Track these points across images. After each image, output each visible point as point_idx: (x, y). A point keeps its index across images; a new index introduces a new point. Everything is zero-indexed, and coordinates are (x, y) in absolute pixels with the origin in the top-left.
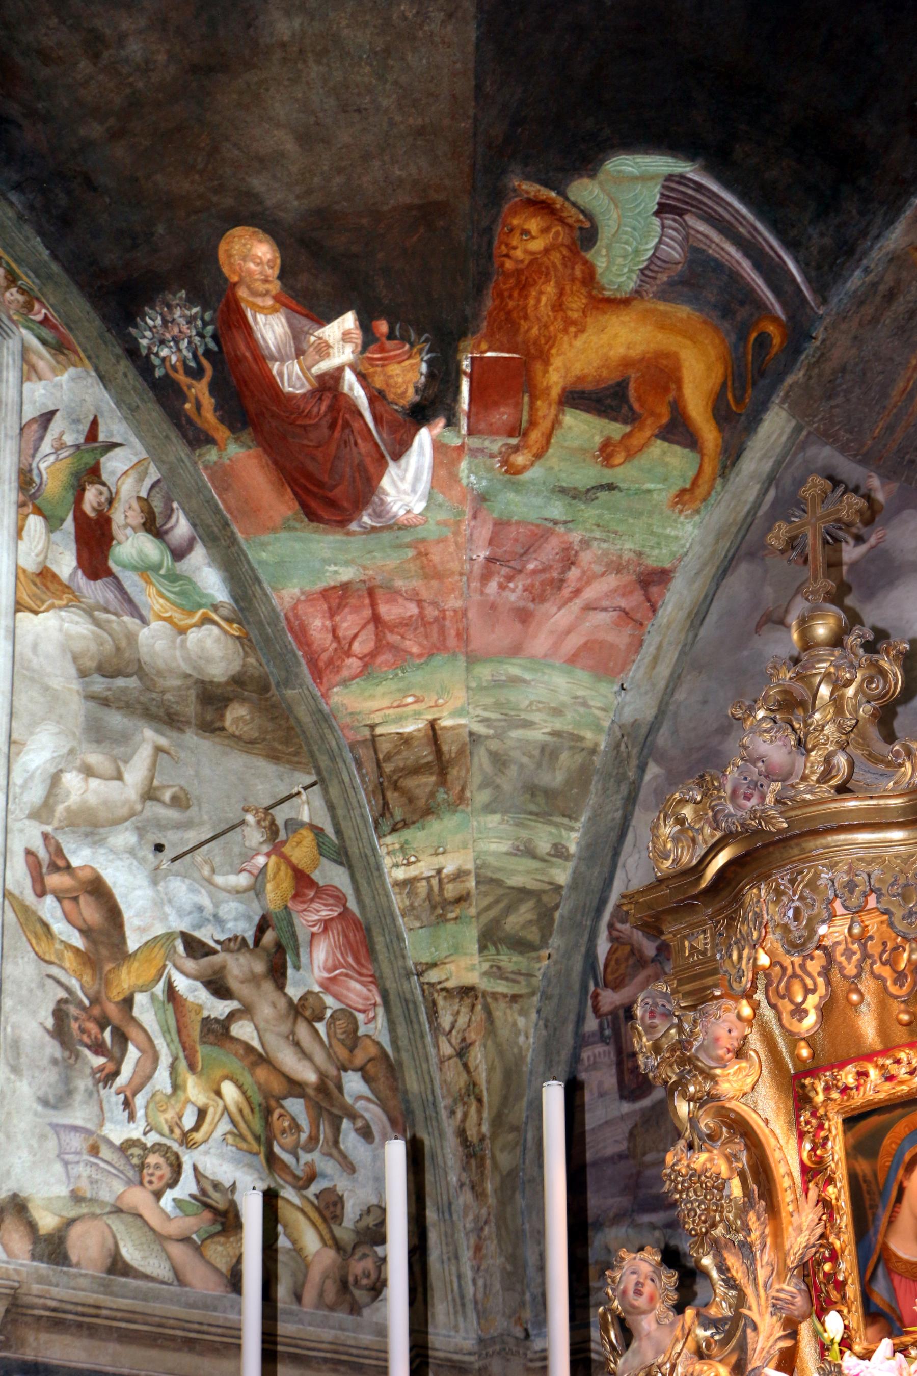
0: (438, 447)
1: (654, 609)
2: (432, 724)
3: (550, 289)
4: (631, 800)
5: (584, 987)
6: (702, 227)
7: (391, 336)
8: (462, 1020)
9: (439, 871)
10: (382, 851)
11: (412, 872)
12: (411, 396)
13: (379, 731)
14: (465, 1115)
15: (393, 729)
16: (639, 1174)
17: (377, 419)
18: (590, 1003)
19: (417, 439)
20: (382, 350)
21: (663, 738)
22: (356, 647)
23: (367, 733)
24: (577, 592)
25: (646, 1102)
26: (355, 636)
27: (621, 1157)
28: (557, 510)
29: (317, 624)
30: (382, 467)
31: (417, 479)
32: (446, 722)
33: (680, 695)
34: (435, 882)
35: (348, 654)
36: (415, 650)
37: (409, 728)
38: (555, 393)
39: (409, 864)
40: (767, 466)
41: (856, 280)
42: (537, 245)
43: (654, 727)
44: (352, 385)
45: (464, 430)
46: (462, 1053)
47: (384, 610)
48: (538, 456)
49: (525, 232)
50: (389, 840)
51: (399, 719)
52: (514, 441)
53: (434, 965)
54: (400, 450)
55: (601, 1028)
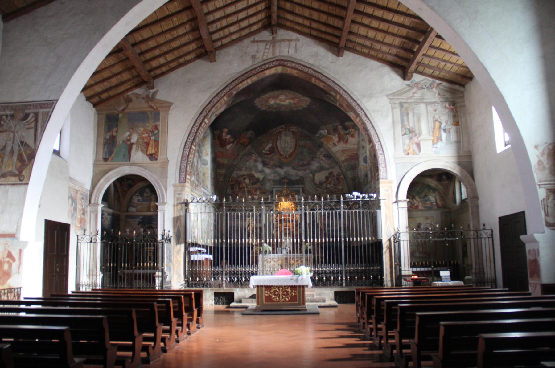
0: (232, 146)
44: (228, 140)
54: (229, 144)
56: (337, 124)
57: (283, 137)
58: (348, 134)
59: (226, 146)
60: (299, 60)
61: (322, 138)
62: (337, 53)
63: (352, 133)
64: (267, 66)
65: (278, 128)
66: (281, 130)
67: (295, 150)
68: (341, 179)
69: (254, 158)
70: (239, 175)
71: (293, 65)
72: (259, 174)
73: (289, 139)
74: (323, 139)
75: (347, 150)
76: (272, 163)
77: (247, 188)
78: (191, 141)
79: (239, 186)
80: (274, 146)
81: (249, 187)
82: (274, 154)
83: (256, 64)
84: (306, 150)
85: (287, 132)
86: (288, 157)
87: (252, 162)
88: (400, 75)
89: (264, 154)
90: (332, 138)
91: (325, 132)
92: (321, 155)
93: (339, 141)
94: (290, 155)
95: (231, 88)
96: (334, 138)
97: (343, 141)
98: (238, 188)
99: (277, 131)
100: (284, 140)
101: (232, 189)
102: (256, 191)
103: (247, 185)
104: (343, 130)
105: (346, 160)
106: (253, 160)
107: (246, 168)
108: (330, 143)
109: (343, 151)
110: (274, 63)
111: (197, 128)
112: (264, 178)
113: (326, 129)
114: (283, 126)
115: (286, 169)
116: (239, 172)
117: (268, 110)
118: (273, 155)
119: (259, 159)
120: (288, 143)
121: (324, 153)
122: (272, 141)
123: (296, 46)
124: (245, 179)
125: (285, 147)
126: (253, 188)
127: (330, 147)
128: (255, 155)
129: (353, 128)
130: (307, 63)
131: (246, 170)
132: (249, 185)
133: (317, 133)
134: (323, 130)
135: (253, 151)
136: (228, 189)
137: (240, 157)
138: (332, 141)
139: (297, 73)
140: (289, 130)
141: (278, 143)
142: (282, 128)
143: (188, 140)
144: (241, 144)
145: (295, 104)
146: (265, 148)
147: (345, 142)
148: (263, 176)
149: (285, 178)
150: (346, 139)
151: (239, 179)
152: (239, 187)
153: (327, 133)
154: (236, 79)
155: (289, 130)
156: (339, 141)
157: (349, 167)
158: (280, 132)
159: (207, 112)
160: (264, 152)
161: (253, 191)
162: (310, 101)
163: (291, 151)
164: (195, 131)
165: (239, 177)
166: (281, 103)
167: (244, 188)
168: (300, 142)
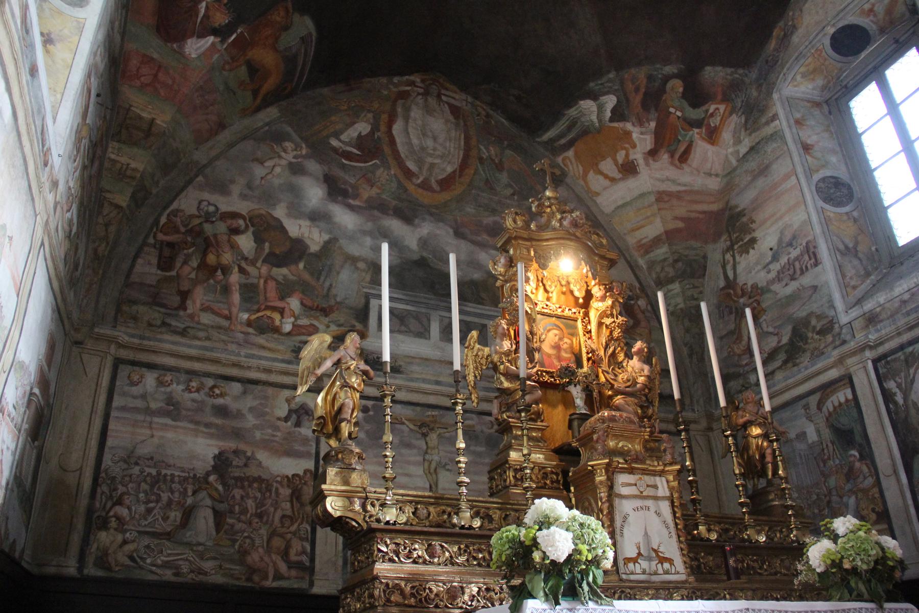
0: (213, 44)
1: (216, 135)
2: (153, 119)
3: (270, 32)
4: (190, 182)
5: (151, 229)
6: (303, 51)
7: (225, 5)
8: (112, 215)
9: (128, 165)
10: (110, 145)
11: (118, 158)
12: (217, 25)
13: (132, 108)
14: (99, 246)
15: (138, 111)
16: (158, 293)
17: (201, 22)
18: (152, 234)
19: (208, 38)
20: (219, 6)
21: (208, 171)
22: (142, 79)
23: (127, 106)
24: (207, 114)
25: (168, 274)
26: (145, 75)
27: (152, 286)
28: (221, 88)
29: (134, 63)
30: (192, 36)
31: (200, 48)
32: (158, 122)
33: (218, 163)
34: (125, 167)
35: (139, 78)
36: (163, 94)
37: (144, 115)
38: (247, 57)
39: (118, 155)
40: (267, 120)
42: (278, 19)
43: (205, 166)
45: (225, 46)
46: (107, 225)
47: (160, 74)
48: (230, 70)
49: (279, 14)
50: (115, 143)
51: (142, 110)
52: (230, 61)
53: (109, 192)
54: (202, 36)
55: (155, 243)
56: (669, 69)
58: (698, 124)
59: (181, 38)
61: (571, 144)
63: (715, 122)
65: (396, 80)
67: (464, 165)
68: (643, 312)
69: (289, 157)
70: (212, 209)
72: (305, 223)
73: (437, 125)
74: (570, 153)
75: (678, 196)
76: (367, 192)
77: (242, 271)
79: (205, 254)
81: (250, 269)
82: (377, 161)
84: (504, 177)
85: (432, 101)
86: (435, 186)
87: (278, 170)
89: (335, 150)
90: (628, 134)
91: (601, 108)
94: (446, 183)
97: (672, 156)
98: (194, 263)
99: (395, 90)
101: (165, 264)
102: (282, 298)
103: (246, 259)
104: (685, 104)
105: (670, 236)
106: (284, 162)
107: (249, 186)
108: (607, 166)
109: (662, 197)
112: (327, 247)
114: (416, 78)
115: (426, 228)
116: (206, 196)
118: (376, 166)
119: (313, 166)
122: (370, 115)
124: (236, 231)
125: (423, 149)
126: (269, 277)
127: (596, 182)
128: (297, 147)
129: (726, 99)
131: (243, 197)
132: (253, 263)
133: (556, 116)
134: (595, 97)
135: (289, 129)
136: (140, 261)
137: (225, 136)
138: (621, 156)
140: (439, 96)
141: (397, 128)
142: (412, 84)
144: (254, 70)
146: (342, 132)
147: (677, 156)
148: (326, 237)
149: (422, 263)
150: (682, 149)
151: (207, 227)
152: (203, 265)
155: (439, 96)
156: (653, 153)
157: (680, 264)
158: (404, 95)
160: (334, 143)
161: (272, 293)
163: (449, 169)
165: (208, 218)
167: (226, 270)
168: (482, 147)
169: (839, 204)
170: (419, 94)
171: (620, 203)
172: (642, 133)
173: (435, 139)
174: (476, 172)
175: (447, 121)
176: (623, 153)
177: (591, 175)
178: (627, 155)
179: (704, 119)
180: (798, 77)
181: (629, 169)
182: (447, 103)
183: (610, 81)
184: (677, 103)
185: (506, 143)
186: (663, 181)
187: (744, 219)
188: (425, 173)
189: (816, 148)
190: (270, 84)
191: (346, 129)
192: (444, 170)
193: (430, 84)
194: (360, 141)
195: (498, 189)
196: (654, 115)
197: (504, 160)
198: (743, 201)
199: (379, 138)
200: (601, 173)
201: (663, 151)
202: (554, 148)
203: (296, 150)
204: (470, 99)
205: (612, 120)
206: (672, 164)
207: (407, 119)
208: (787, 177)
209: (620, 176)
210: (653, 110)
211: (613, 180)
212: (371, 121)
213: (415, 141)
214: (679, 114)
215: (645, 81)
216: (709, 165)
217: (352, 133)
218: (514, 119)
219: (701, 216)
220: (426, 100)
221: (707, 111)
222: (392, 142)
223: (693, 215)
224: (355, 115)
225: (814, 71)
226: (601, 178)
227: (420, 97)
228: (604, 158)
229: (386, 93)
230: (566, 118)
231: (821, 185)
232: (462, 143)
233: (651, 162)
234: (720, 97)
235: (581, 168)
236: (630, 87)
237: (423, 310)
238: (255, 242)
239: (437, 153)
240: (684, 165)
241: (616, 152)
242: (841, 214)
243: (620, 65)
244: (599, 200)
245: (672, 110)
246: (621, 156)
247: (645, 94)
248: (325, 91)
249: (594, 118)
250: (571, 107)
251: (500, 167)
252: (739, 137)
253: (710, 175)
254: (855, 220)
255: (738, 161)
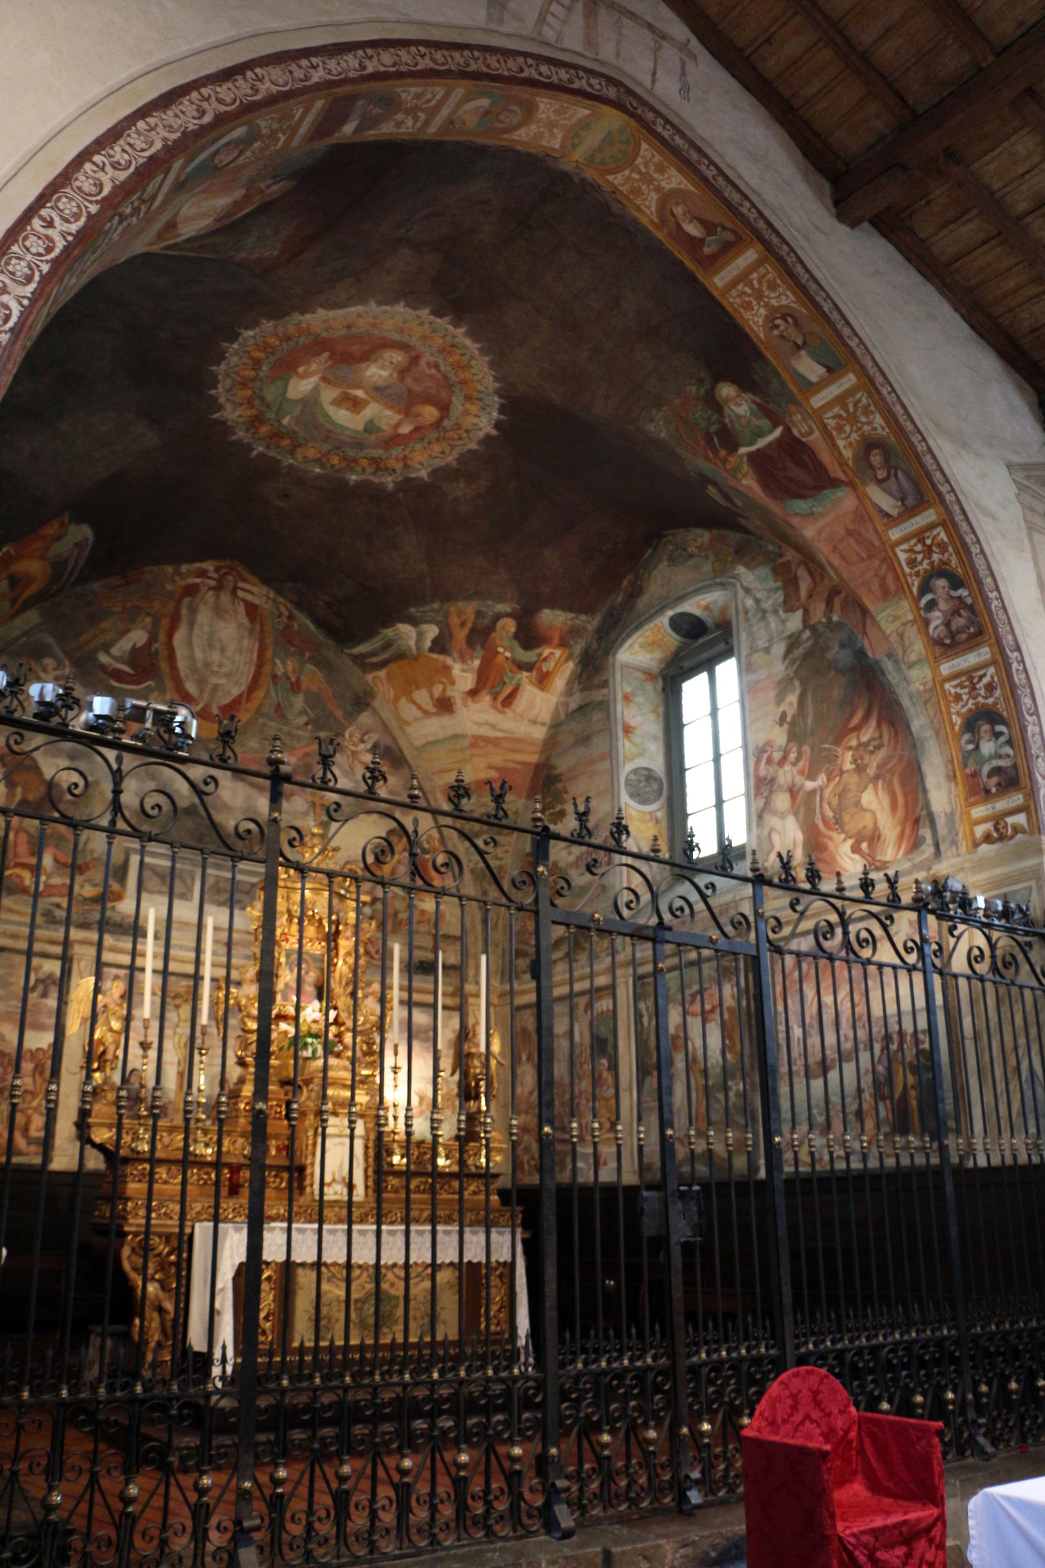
41: (78, 589)
56: (501, 607)
57: (204, 616)
58: (529, 667)
60: (702, 138)
61: (383, 664)
62: (830, 202)
64: (563, 75)
65: (184, 568)
66: (198, 580)
67: (253, 686)
71: (679, 141)
74: (382, 673)
75: (496, 742)
78: (60, 244)
80: (156, 646)
82: (150, 683)
83: (508, 35)
84: (299, 701)
85: (225, 598)
88: (1030, 405)
89: (103, 668)
90: (447, 669)
91: (420, 636)
92: (362, 741)
93: (473, 693)
95: (370, 69)
96: (457, 669)
97: (495, 699)
99: (182, 583)
100: (206, 629)
104: (516, 645)
108: (422, 696)
109: (478, 742)
110: (594, 82)
111: (122, 176)
113: (437, 623)
114: (209, 566)
117: (241, 434)
120: (223, 650)
121: (373, 738)
122: (148, 620)
123: (683, 73)
125: (207, 665)
127: (407, 710)
128: (59, 665)
129: (563, 644)
130: (733, 168)
133: (369, 633)
134: (414, 622)
135: (50, 640)
138: (437, 690)
139: (666, 198)
140: (234, 592)
141: (179, 638)
142: (203, 574)
143: (36, 223)
145: (395, 440)
153: (428, 644)
154: (404, 43)
155: (234, 592)
156: (473, 693)
158: (191, 591)
159: (207, 119)
160: (103, 658)
162: (473, 446)
163: (235, 692)
164: (100, 186)
166: (331, 410)
168: (278, 661)
169: (644, 802)
170: (210, 588)
171: (431, 739)
172: (463, 671)
173: (223, 650)
174: (267, 694)
175: (240, 626)
176: (440, 687)
177: (403, 702)
178: (444, 690)
179: (535, 663)
180: (636, 647)
181: (445, 705)
182: (244, 601)
183: (433, 610)
184: (506, 643)
185: (307, 654)
186: (480, 725)
187: (559, 786)
188: (206, 697)
189: (638, 732)
190: (32, 589)
191: (119, 639)
192: (229, 693)
193: (226, 574)
194: (135, 656)
195: (290, 717)
196: (479, 652)
197: (302, 678)
198: (563, 764)
199: (157, 651)
200: (414, 702)
201: (484, 693)
202: (364, 663)
203: (56, 669)
204: (272, 594)
205: (431, 650)
206: (494, 707)
207: (192, 623)
208: (602, 758)
209: (433, 710)
210: (478, 647)
211: (426, 712)
212: (149, 627)
213: (199, 655)
214: (508, 654)
215: (472, 617)
216: (535, 712)
217: (124, 646)
218: (321, 623)
219: (519, 767)
220: (218, 597)
221: (540, 655)
222: (172, 656)
223: (512, 765)
224: (131, 618)
225: (653, 644)
226: (414, 708)
227: (211, 593)
228: (418, 687)
229: (169, 587)
230: (380, 637)
231: (633, 777)
232: (255, 655)
233: (470, 702)
234: (556, 641)
235: (392, 692)
236: (455, 621)
237: (188, 867)
238: (7, 786)
239: (225, 670)
240: (507, 710)
241: (432, 684)
242: (644, 813)
243: (446, 598)
244: (409, 730)
245: (500, 650)
246: (437, 690)
247: (472, 630)
248: (97, 586)
249: (412, 643)
250: (387, 627)
251: (295, 687)
252: (572, 688)
253: (535, 723)
254: (657, 821)
255: (567, 715)
